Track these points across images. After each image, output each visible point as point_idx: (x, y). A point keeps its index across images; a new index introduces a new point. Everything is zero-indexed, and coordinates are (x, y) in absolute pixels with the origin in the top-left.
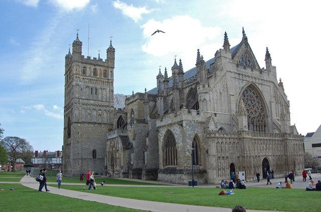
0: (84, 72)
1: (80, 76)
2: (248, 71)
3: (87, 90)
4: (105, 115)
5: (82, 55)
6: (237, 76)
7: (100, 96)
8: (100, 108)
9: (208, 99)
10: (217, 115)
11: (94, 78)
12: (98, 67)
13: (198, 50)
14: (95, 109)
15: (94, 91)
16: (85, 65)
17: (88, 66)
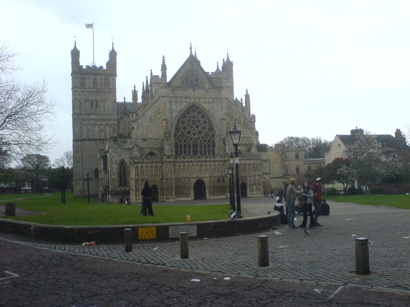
0: (83, 85)
1: (79, 90)
2: (190, 92)
3: (88, 103)
4: (108, 129)
5: (81, 64)
6: (173, 99)
7: (102, 109)
8: (101, 122)
9: (135, 127)
10: (146, 141)
11: (94, 90)
12: (98, 77)
13: (151, 70)
14: (95, 125)
15: (94, 104)
16: (83, 76)
17: (87, 77)
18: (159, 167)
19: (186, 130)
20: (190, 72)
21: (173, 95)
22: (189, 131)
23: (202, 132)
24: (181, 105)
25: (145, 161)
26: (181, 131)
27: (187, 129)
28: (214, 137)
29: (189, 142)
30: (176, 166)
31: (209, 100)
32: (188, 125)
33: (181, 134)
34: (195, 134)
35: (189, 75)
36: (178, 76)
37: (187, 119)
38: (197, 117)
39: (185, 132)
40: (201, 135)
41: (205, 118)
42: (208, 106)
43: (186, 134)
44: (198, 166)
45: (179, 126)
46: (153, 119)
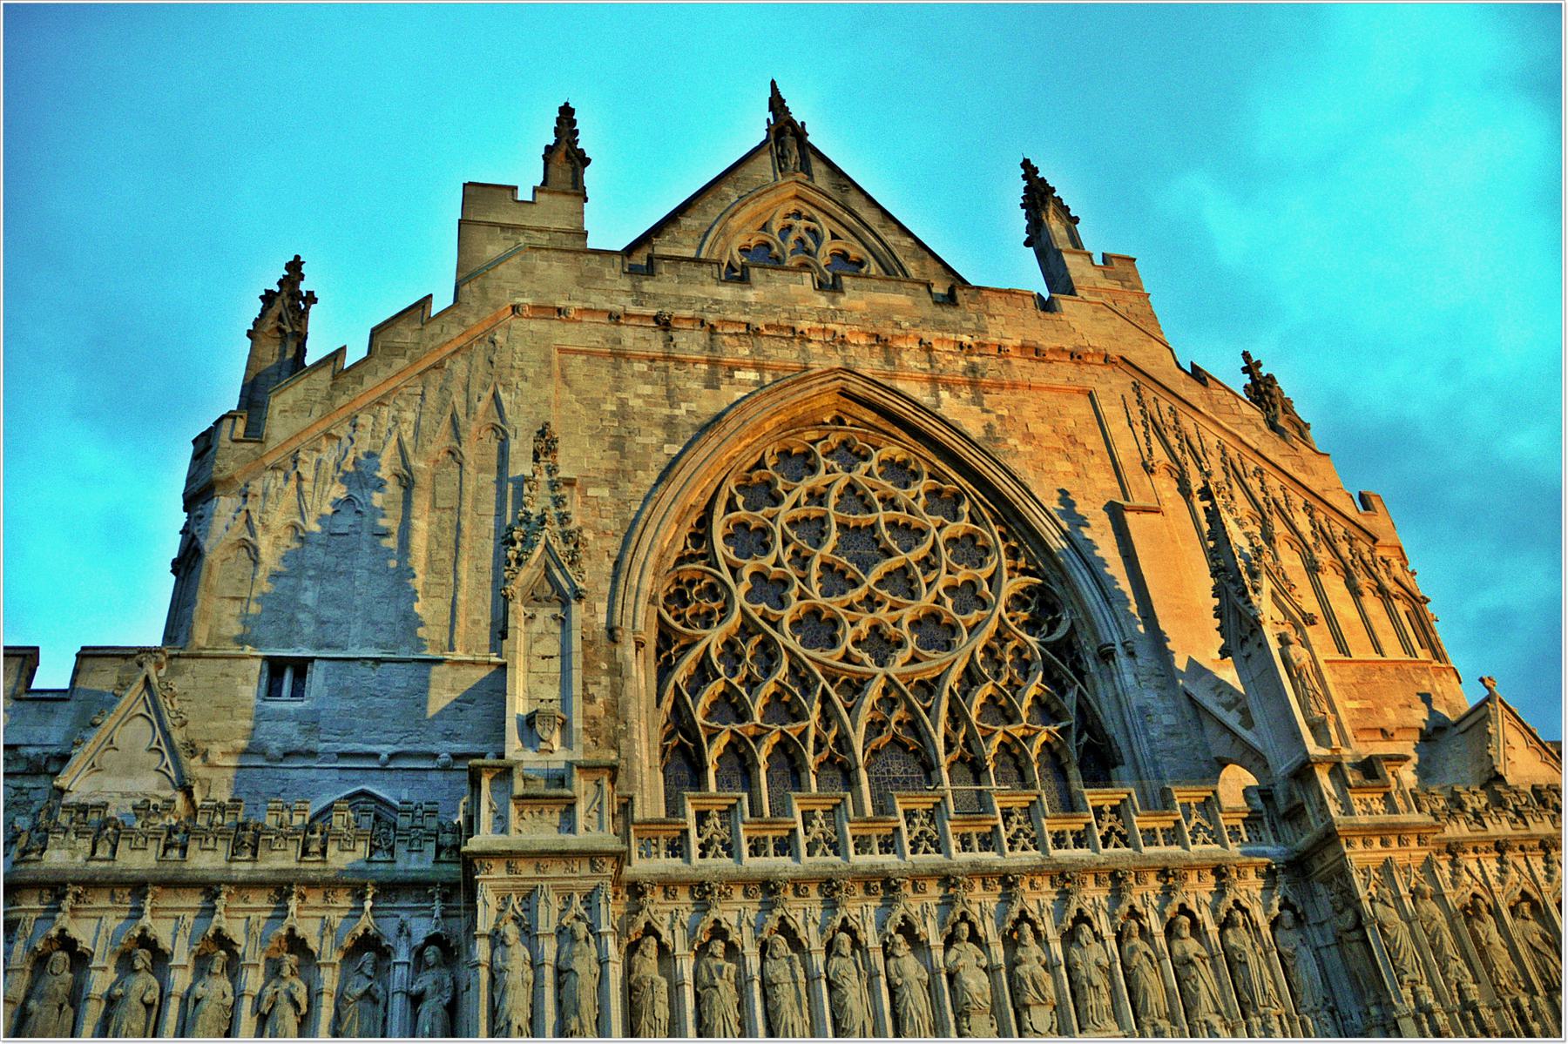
18: (403, 955)
19: (782, 603)
20: (788, 216)
21: (635, 303)
22: (815, 612)
23: (953, 629)
24: (712, 383)
25: (206, 860)
26: (735, 618)
27: (793, 593)
28: (1080, 675)
29: (827, 718)
30: (663, 950)
31: (973, 369)
32: (801, 560)
33: (729, 644)
34: (882, 643)
35: (776, 229)
36: (685, 221)
37: (785, 512)
38: (890, 503)
39: (775, 625)
40: (945, 657)
41: (965, 508)
42: (976, 409)
43: (788, 639)
44: (974, 937)
45: (709, 564)
46: (419, 479)
